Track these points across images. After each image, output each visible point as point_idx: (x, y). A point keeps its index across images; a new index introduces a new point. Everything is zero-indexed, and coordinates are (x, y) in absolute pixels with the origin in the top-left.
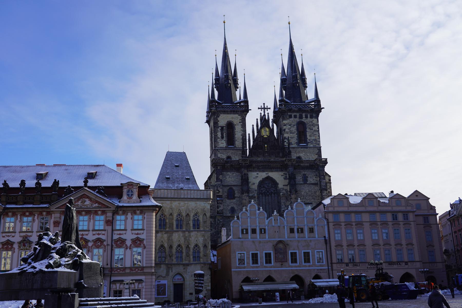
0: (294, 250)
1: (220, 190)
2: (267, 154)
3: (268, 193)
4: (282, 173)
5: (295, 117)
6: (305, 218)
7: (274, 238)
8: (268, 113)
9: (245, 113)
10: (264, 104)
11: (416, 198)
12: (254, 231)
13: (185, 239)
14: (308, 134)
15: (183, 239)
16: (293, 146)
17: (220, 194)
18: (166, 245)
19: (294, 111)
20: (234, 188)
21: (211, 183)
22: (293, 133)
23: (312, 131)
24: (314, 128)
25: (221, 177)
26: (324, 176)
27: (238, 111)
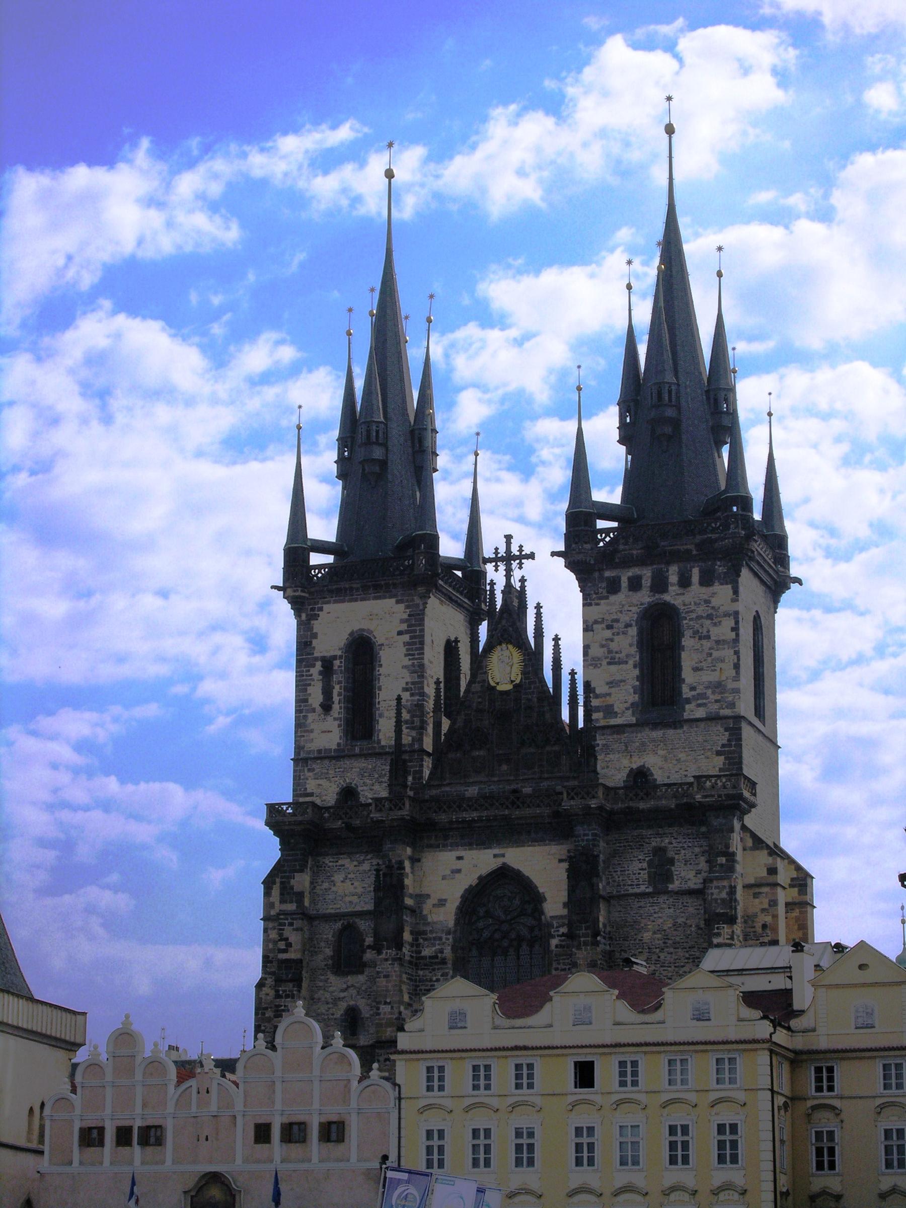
1: (294, 938)
2: (505, 767)
3: (505, 943)
5: (635, 584)
6: (316, 1084)
8: (523, 580)
9: (421, 589)
10: (508, 538)
12: (124, 1136)
14: (687, 661)
17: (292, 955)
19: (627, 563)
20: (364, 925)
22: (620, 663)
24: (715, 632)
26: (731, 857)
27: (394, 585)
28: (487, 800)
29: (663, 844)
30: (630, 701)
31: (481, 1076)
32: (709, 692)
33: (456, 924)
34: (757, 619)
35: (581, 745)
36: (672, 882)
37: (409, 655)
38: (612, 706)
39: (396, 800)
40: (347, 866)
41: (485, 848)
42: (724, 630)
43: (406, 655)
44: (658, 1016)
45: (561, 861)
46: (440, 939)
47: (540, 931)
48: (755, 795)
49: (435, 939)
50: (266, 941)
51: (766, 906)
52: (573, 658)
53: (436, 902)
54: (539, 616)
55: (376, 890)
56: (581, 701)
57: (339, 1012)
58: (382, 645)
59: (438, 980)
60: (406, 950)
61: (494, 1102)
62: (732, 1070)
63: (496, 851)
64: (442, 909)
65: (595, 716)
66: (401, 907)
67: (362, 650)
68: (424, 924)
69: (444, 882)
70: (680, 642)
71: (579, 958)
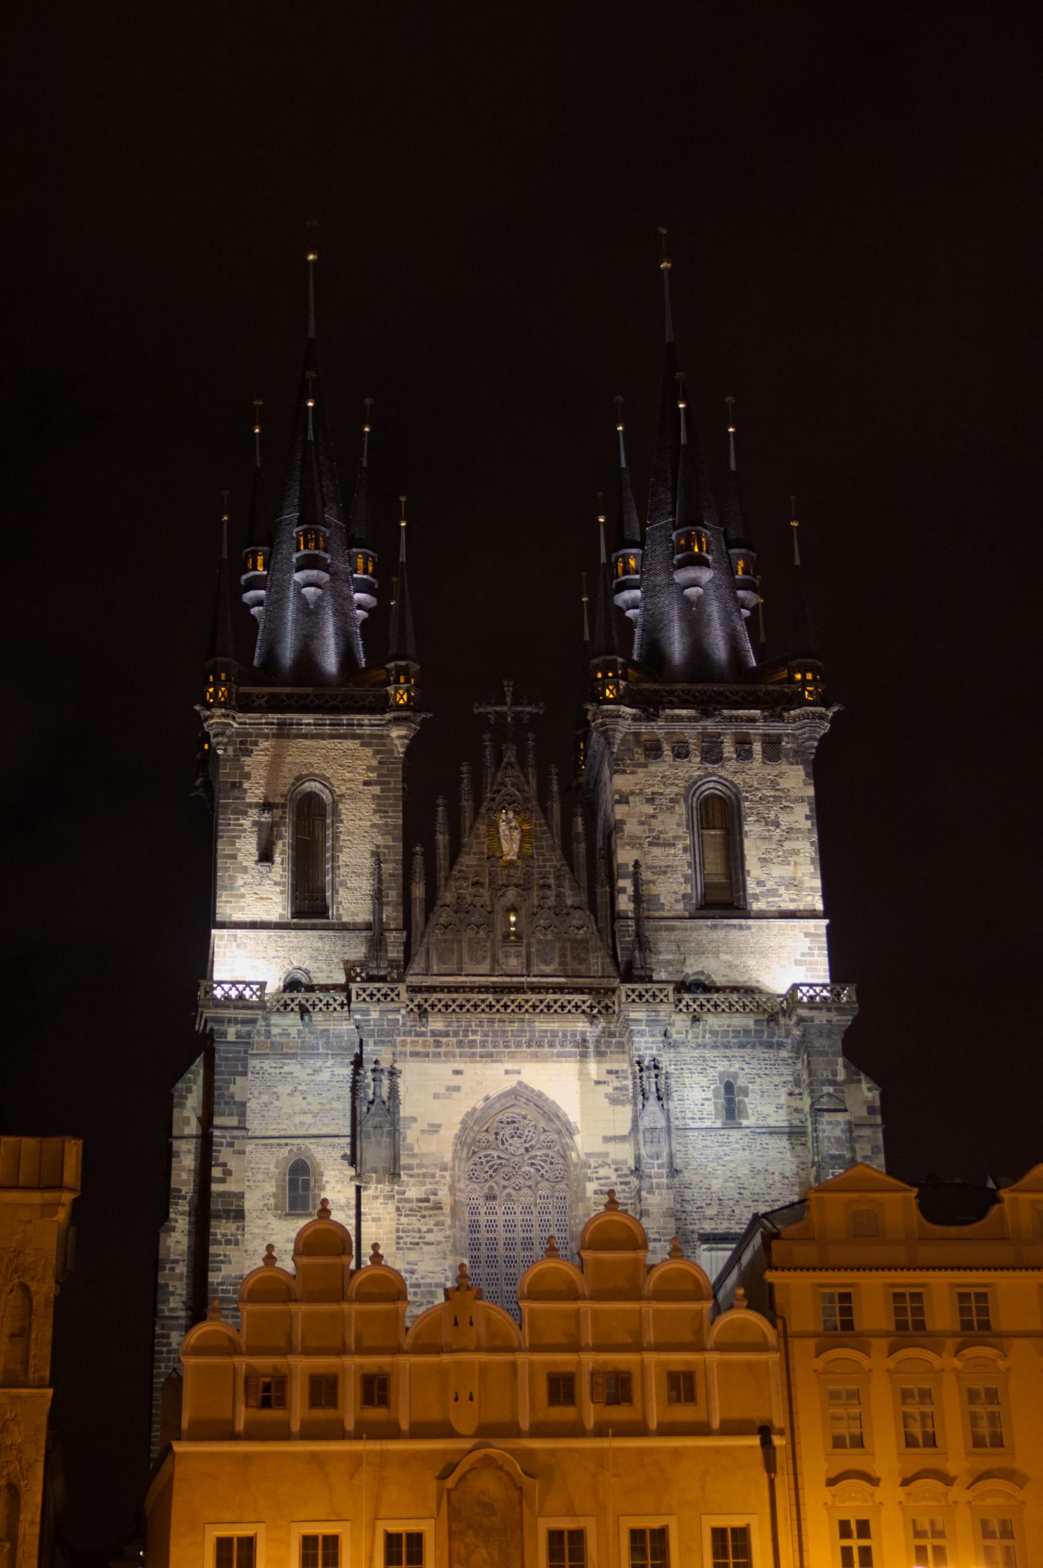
0: (571, 1513)
5: (681, 752)
7: (451, 1433)
12: (324, 1390)
14: (752, 851)
17: (231, 1186)
21: (186, 1121)
24: (785, 819)
29: (732, 1070)
30: (681, 893)
32: (782, 890)
33: (454, 1159)
36: (747, 1118)
37: (380, 811)
38: (658, 895)
40: (295, 1075)
41: (492, 1062)
43: (375, 812)
45: (598, 1083)
46: (433, 1176)
49: (424, 1175)
51: (869, 1153)
53: (426, 1127)
58: (342, 796)
59: (429, 1231)
63: (509, 1066)
64: (435, 1137)
68: (409, 1155)
69: (436, 1101)
70: (741, 827)
71: (651, 1205)
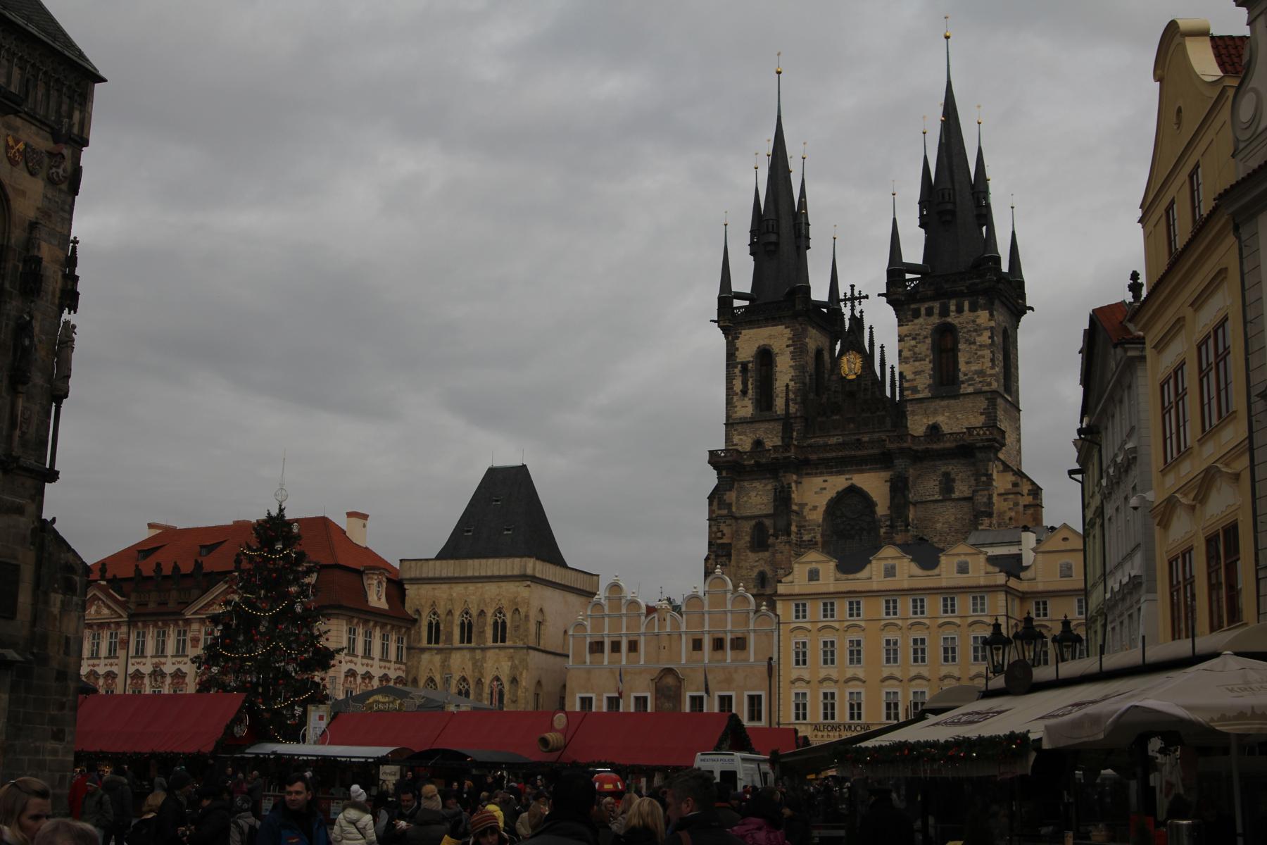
1: (726, 530)
4: (886, 475)
5: (929, 312)
8: (861, 312)
10: (852, 286)
11: (1063, 546)
12: (616, 647)
13: (474, 664)
14: (962, 359)
15: (470, 664)
16: (921, 396)
17: (724, 541)
18: (437, 678)
19: (923, 300)
20: (768, 522)
23: (974, 347)
25: (731, 496)
26: (990, 477)
28: (842, 445)
31: (828, 610)
34: (1005, 331)
35: (898, 411)
39: (786, 446)
42: (985, 338)
44: (936, 571)
47: (874, 524)
48: (1004, 438)
50: (710, 533)
52: (892, 359)
54: (871, 333)
55: (775, 500)
56: (898, 384)
57: (754, 574)
60: (793, 537)
61: (836, 625)
62: (983, 604)
65: (906, 393)
66: (790, 511)
67: (765, 356)
